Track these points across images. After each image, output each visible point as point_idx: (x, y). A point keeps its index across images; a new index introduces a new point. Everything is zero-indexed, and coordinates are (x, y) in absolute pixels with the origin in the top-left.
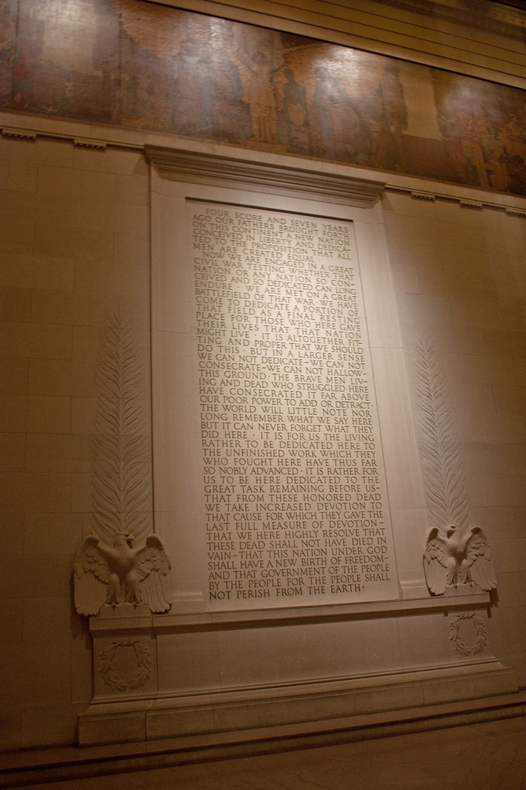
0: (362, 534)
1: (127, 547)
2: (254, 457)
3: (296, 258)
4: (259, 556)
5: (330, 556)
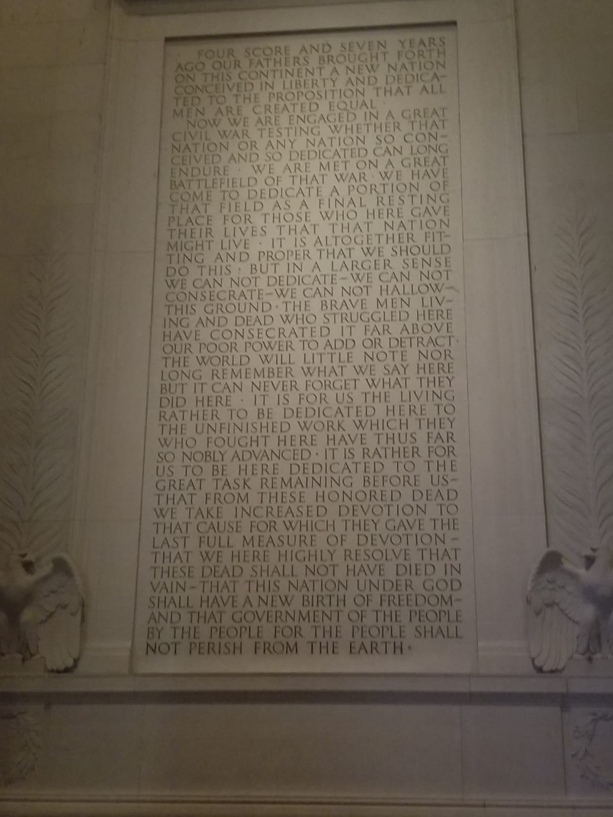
0: (415, 558)
1: (21, 571)
2: (238, 434)
3: (342, 106)
4: (231, 589)
5: (352, 591)
